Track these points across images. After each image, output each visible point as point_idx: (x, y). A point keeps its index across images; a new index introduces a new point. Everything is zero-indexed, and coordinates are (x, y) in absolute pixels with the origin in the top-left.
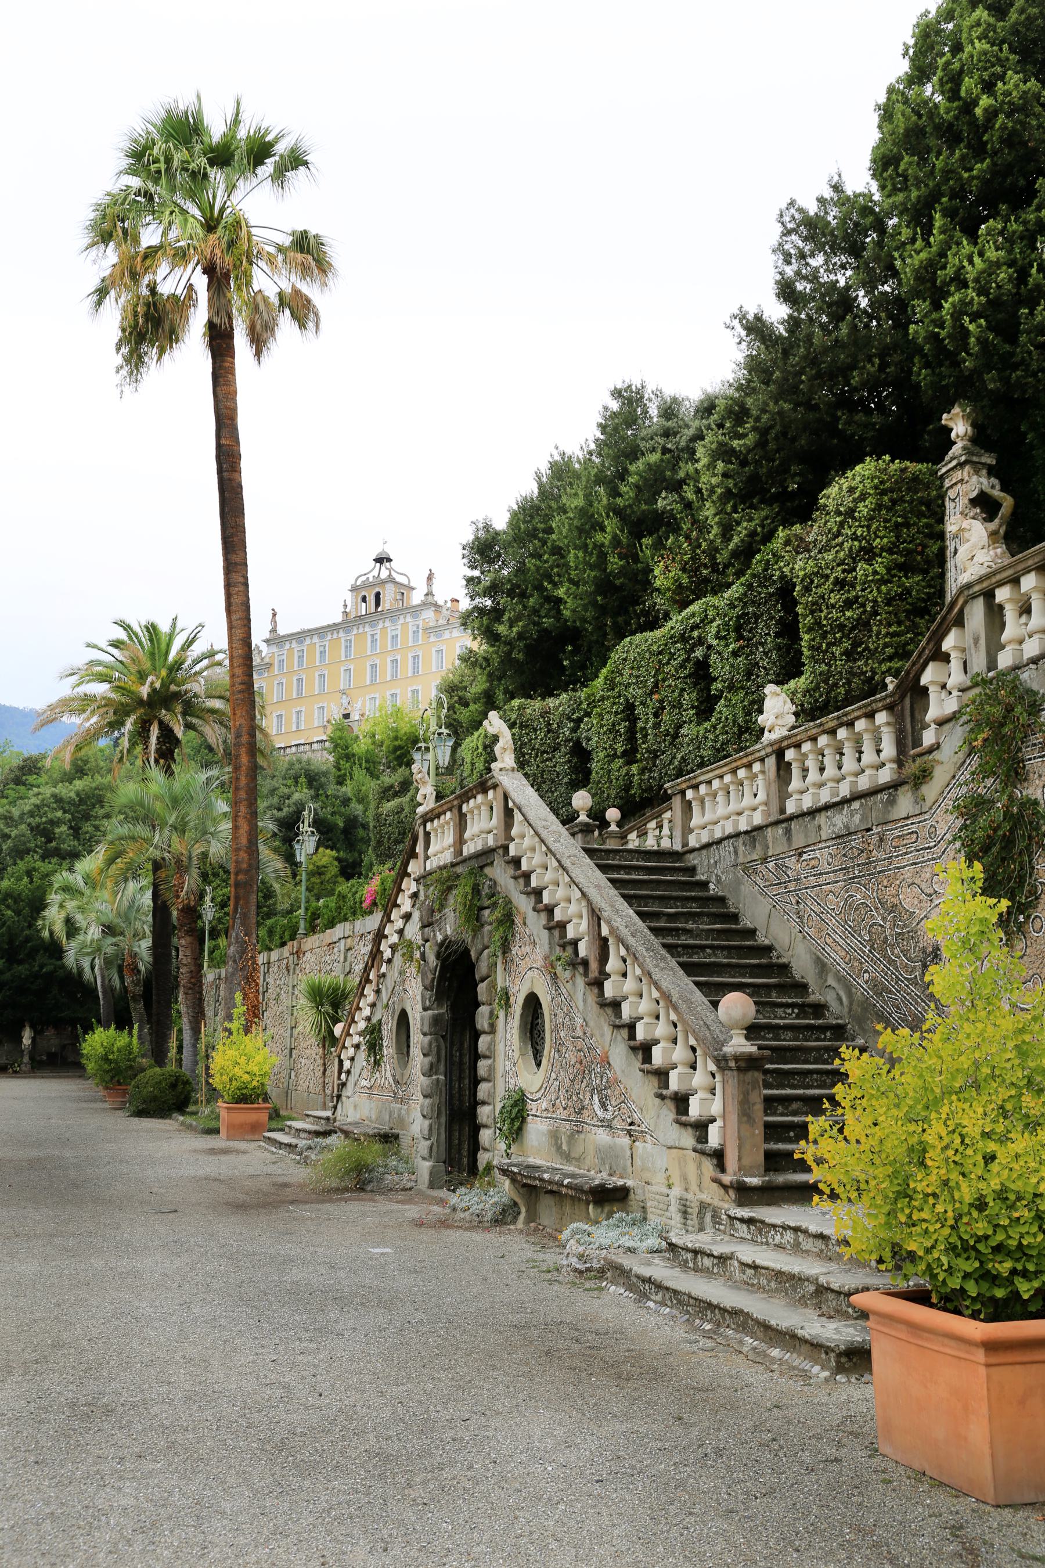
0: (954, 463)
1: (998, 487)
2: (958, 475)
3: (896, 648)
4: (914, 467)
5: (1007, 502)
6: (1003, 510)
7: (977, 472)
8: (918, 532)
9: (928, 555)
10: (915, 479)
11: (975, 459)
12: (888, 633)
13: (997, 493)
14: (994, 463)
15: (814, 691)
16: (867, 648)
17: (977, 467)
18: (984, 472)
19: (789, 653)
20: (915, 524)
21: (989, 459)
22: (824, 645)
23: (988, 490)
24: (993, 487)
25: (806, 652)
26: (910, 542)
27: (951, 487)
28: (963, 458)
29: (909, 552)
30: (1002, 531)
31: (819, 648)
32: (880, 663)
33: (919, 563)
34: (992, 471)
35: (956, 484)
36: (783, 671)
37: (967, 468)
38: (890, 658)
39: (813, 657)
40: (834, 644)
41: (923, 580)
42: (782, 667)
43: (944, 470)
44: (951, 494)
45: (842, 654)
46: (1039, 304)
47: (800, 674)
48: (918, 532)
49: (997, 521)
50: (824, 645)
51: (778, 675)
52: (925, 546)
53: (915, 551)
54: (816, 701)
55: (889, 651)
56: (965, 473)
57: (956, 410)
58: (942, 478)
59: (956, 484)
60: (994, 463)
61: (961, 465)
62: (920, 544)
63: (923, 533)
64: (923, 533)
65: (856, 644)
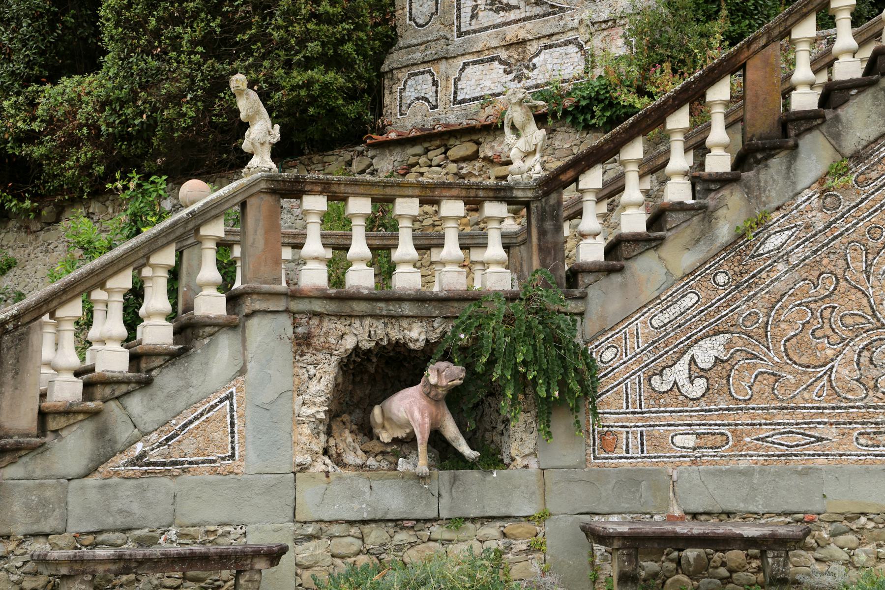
3: (323, 45)
12: (313, 15)
15: (123, 103)
16: (263, 37)
19: (53, 29)
22: (153, 22)
25: (109, 29)
31: (138, 26)
32: (288, 65)
36: (41, 60)
38: (308, 64)
39: (123, 40)
40: (178, 21)
42: (42, 53)
45: (193, 43)
47: (94, 67)
50: (153, 22)
51: (30, 65)
54: (125, 123)
55: (314, 47)
65: (231, 27)
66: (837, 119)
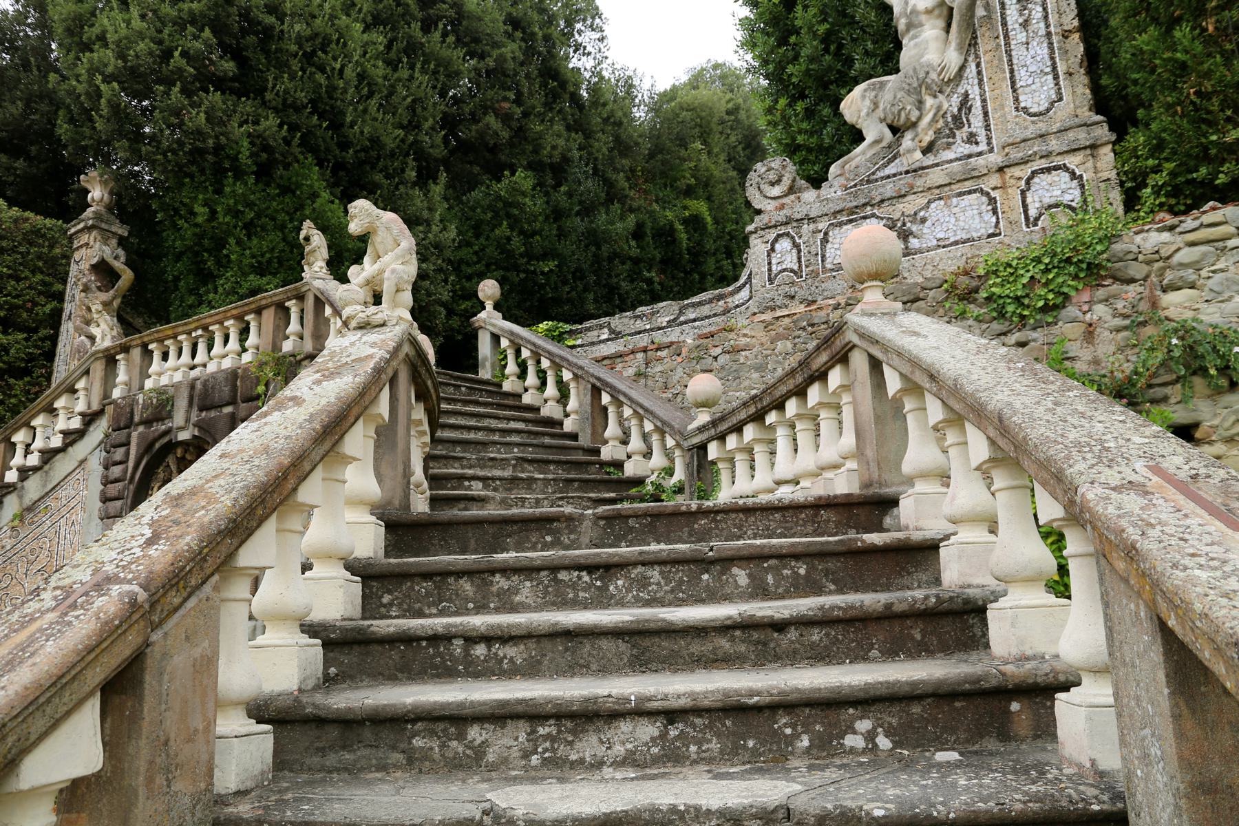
0: (81, 225)
1: (123, 259)
2: (85, 238)
4: (38, 220)
5: (127, 276)
6: (120, 283)
7: (105, 241)
8: (30, 287)
9: (37, 314)
10: (37, 232)
11: (103, 226)
13: (118, 265)
14: (126, 234)
17: (106, 236)
18: (114, 242)
20: (26, 278)
21: (123, 231)
23: (110, 260)
24: (116, 258)
26: (17, 297)
27: (78, 249)
28: (90, 222)
29: (13, 307)
30: (116, 304)
33: (26, 321)
34: (122, 242)
35: (81, 247)
37: (94, 233)
41: (26, 339)
43: (73, 230)
44: (77, 256)
46: (174, 85)
48: (30, 287)
49: (112, 292)
52: (35, 304)
53: (22, 307)
56: (92, 238)
57: (93, 173)
58: (71, 239)
59: (81, 247)
60: (126, 234)
61: (88, 229)
62: (29, 301)
63: (35, 289)
64: (35, 289)
66: (23, 487)
